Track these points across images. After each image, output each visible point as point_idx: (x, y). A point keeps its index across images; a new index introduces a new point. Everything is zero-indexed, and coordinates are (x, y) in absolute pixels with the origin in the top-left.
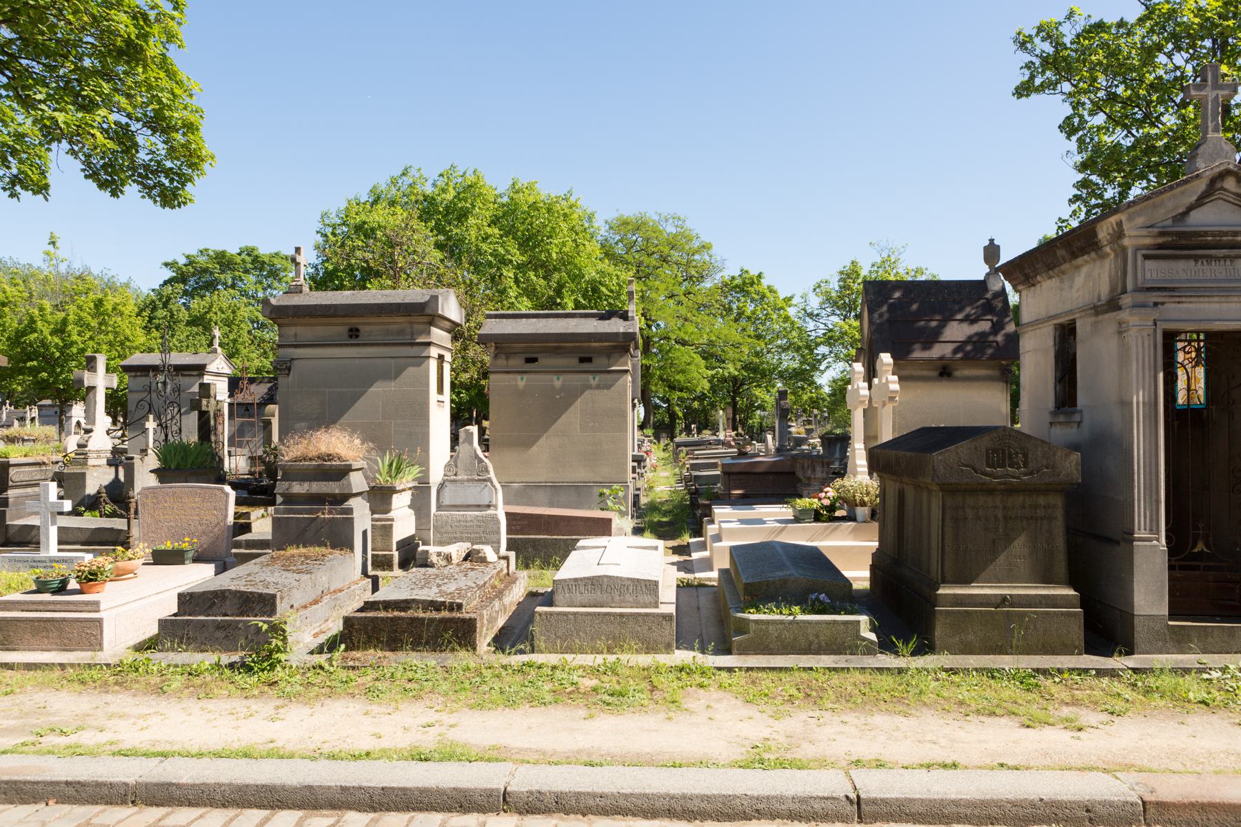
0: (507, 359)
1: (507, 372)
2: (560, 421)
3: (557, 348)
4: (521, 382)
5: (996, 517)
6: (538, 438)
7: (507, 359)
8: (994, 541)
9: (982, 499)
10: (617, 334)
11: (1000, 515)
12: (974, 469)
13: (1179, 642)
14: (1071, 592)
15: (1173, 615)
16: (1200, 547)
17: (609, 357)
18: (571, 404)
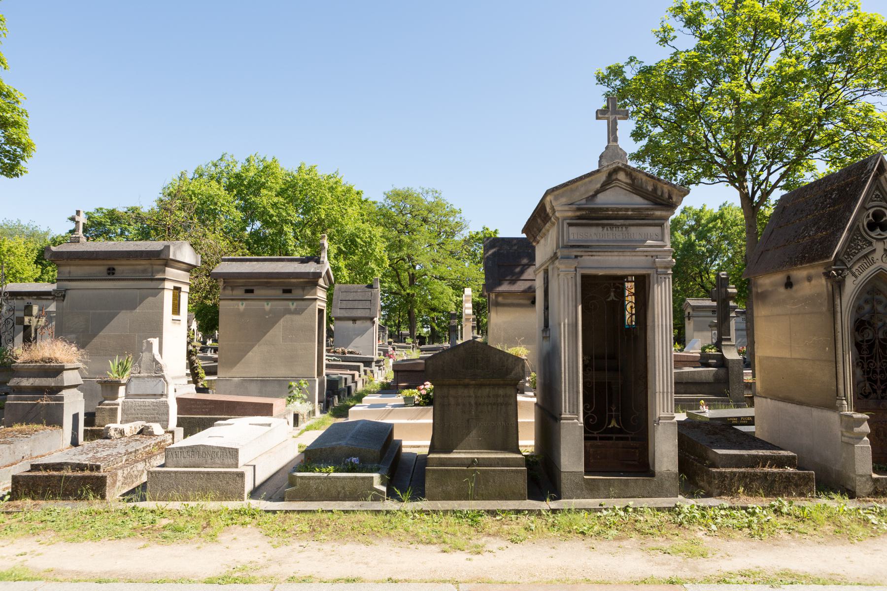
0: (232, 290)
1: (232, 300)
3: (267, 283)
4: (241, 306)
5: (470, 403)
6: (252, 346)
7: (232, 290)
8: (468, 420)
9: (461, 391)
10: (308, 273)
11: (473, 402)
13: (591, 490)
15: (587, 472)
16: (613, 424)
17: (303, 288)
18: (276, 322)
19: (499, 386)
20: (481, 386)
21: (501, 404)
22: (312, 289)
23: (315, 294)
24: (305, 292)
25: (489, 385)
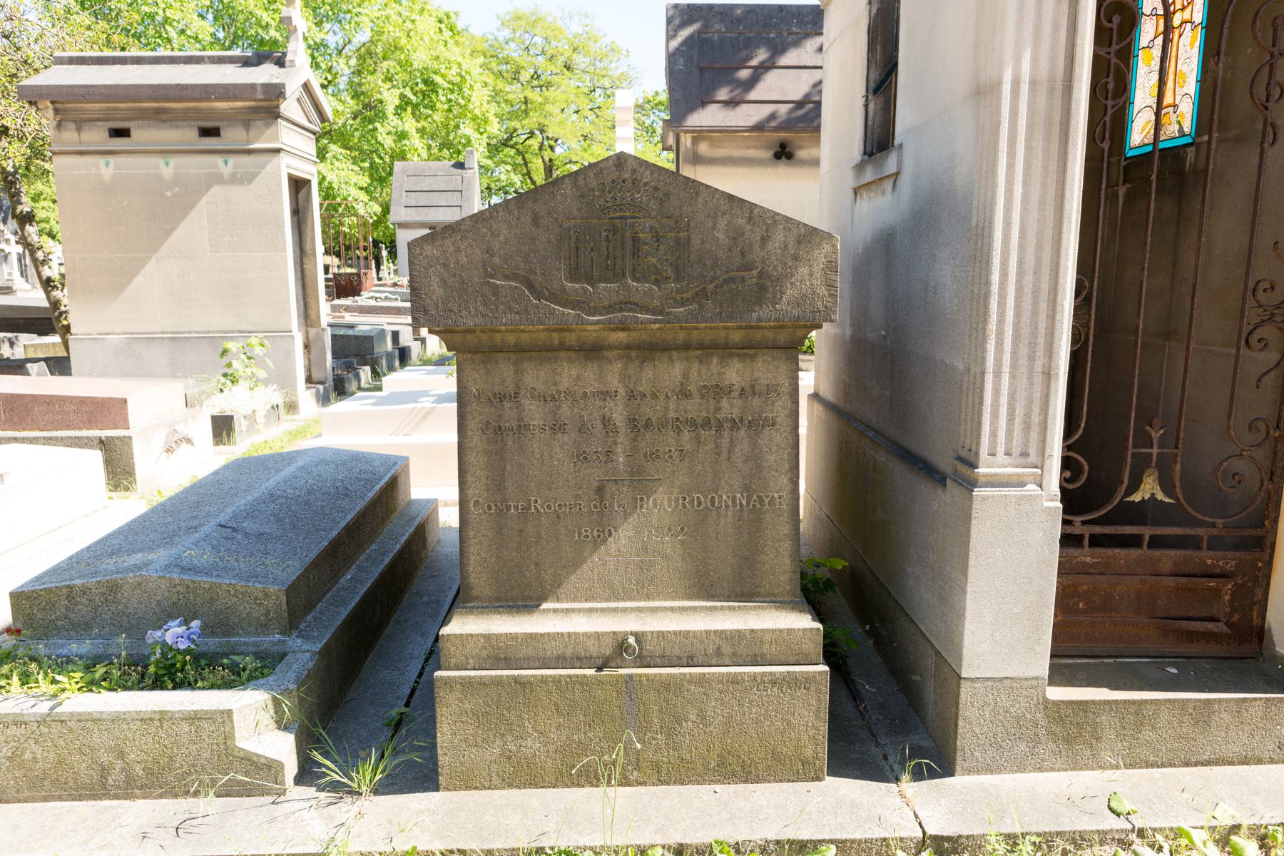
0: (79, 129)
1: (81, 153)
2: (176, 233)
4: (106, 168)
5: (606, 421)
6: (142, 264)
7: (79, 129)
8: (600, 490)
9: (568, 374)
11: (619, 415)
12: (530, 286)
13: (1068, 742)
14: (804, 622)
15: (1059, 675)
16: (1149, 488)
17: (247, 125)
18: (192, 206)
19: (724, 349)
20: (651, 350)
21: (735, 425)
22: (268, 126)
23: (276, 138)
24: (253, 132)
25: (686, 347)
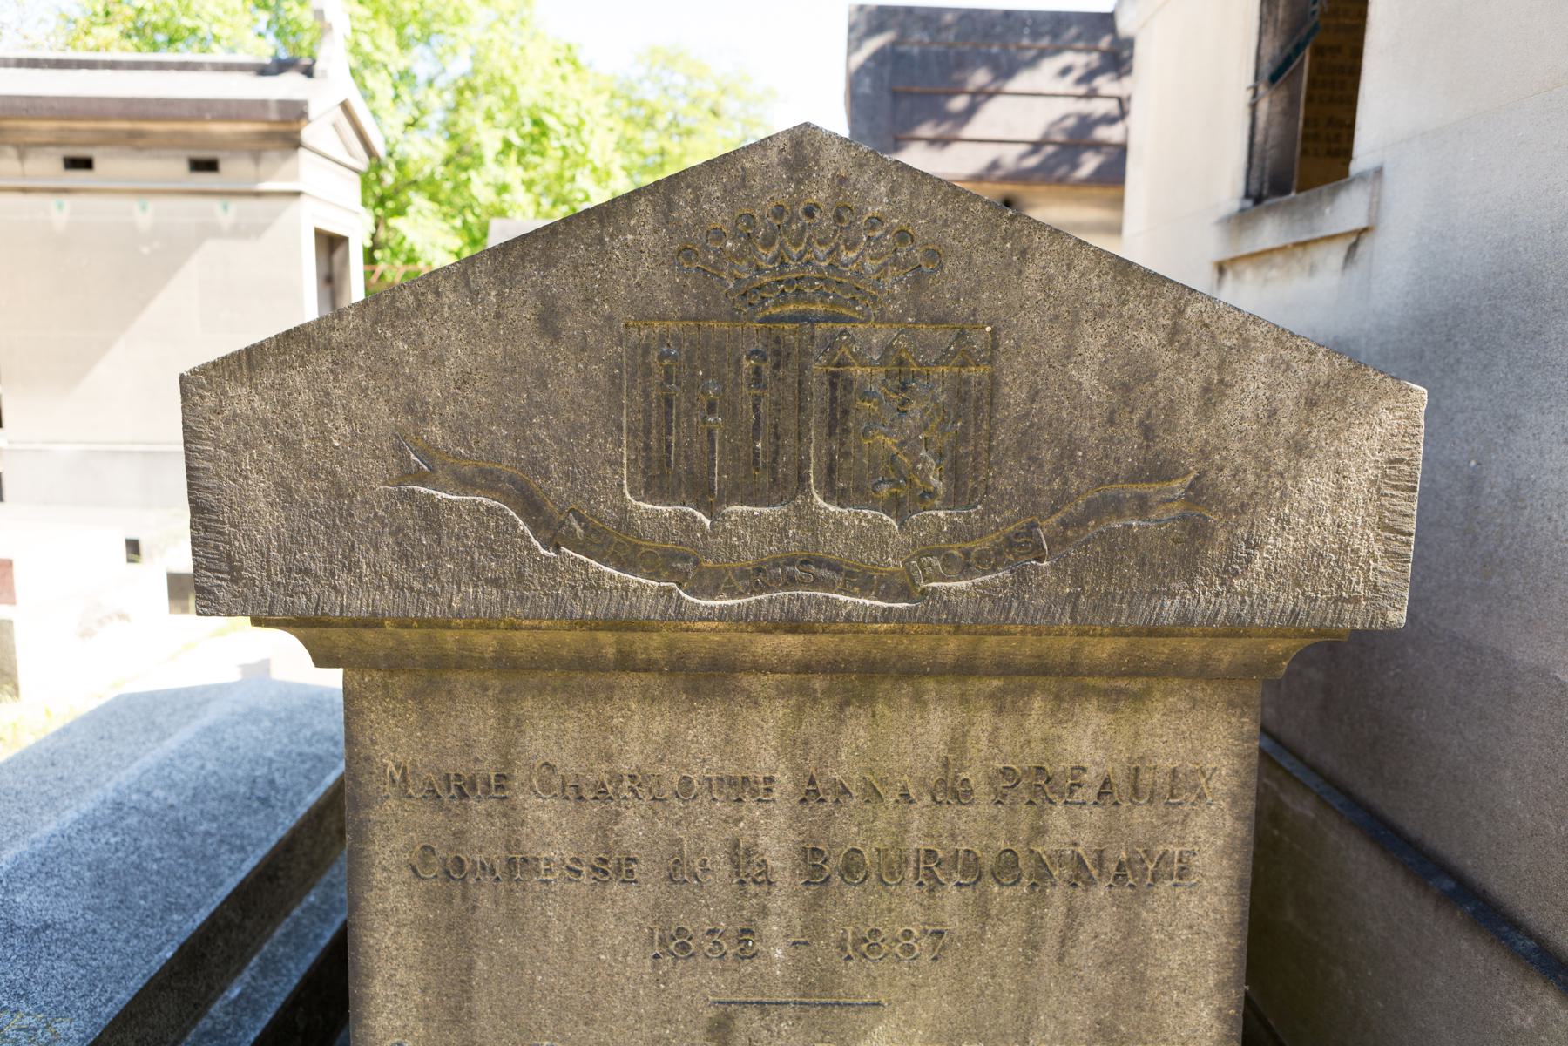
0: (22, 157)
1: (24, 190)
4: (59, 212)
5: (741, 856)
7: (22, 157)
9: (642, 731)
10: (264, 104)
11: (775, 840)
12: (531, 506)
17: (256, 156)
19: (1066, 679)
20: (862, 677)
21: (1081, 874)
22: (285, 158)
23: (295, 176)
24: (264, 167)
25: (964, 669)
